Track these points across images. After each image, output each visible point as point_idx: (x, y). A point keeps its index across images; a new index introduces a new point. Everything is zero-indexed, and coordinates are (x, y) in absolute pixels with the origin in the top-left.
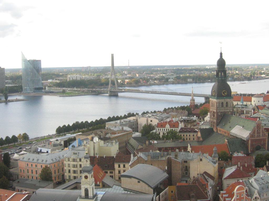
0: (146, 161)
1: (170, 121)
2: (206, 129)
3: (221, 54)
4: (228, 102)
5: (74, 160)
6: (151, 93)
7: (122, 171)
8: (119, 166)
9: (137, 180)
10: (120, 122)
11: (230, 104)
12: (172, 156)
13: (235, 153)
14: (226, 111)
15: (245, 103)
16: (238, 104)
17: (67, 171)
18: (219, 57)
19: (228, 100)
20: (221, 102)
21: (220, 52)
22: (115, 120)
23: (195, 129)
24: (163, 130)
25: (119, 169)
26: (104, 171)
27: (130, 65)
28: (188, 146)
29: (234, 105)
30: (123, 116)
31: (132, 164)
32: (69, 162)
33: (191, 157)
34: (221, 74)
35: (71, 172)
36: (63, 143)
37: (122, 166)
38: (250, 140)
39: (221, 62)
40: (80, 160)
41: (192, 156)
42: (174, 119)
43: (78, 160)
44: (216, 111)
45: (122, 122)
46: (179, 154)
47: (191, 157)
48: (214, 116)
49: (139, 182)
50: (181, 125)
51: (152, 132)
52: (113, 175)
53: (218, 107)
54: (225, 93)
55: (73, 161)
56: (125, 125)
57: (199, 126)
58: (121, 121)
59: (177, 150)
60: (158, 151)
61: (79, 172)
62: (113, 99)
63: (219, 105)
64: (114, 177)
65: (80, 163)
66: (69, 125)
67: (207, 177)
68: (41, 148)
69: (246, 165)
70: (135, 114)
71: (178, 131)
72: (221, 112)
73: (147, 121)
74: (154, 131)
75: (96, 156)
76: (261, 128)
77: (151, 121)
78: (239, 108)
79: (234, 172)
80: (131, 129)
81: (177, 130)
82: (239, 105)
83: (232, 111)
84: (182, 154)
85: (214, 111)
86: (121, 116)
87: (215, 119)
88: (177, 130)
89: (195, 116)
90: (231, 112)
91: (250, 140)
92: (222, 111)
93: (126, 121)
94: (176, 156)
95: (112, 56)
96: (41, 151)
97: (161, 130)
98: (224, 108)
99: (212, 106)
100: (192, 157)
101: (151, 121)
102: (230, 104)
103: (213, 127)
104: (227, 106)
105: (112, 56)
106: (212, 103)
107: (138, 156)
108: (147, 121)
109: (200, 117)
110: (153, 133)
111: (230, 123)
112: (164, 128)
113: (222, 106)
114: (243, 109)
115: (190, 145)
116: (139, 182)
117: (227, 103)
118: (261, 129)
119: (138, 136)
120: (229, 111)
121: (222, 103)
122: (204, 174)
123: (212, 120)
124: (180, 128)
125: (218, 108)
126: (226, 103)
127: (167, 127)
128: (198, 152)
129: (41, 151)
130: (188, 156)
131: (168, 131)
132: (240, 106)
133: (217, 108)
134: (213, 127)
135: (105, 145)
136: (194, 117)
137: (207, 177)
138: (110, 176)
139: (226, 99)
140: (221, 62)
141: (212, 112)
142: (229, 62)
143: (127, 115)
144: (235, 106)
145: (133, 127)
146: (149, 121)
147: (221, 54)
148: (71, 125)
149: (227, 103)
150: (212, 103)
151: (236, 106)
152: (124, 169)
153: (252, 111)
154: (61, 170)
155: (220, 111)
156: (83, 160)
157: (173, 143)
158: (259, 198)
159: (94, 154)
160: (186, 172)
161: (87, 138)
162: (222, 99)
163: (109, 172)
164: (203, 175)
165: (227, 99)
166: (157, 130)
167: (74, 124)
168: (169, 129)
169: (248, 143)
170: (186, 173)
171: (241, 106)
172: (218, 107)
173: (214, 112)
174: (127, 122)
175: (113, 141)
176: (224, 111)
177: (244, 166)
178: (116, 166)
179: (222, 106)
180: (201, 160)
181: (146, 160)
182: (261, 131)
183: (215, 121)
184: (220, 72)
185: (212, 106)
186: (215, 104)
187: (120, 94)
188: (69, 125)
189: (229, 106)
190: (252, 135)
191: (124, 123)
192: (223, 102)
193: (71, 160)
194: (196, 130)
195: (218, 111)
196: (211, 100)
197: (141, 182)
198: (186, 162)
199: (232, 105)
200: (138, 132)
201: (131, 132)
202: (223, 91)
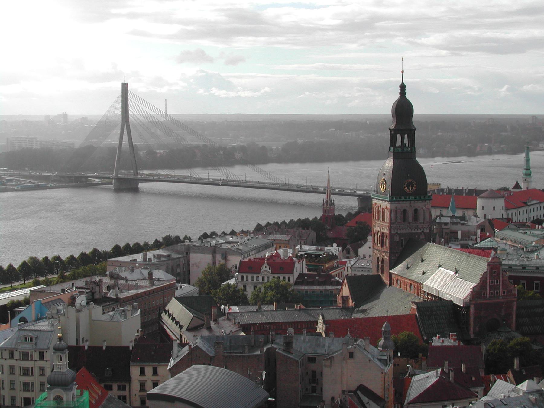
0: (211, 358)
1: (271, 257)
2: (362, 276)
3: (403, 87)
4: (419, 209)
5: (26, 356)
6: (222, 185)
7: (149, 384)
8: (142, 372)
10: (145, 259)
11: (424, 214)
12: (278, 346)
13: (434, 338)
14: (413, 231)
15: (459, 213)
16: (441, 216)
18: (397, 96)
19: (419, 205)
20: (402, 210)
21: (400, 84)
22: (131, 254)
23: (333, 277)
24: (253, 280)
25: (143, 378)
26: (102, 385)
27: (171, 111)
28: (318, 319)
29: (434, 216)
30: (151, 242)
31: (175, 366)
32: (12, 362)
33: (326, 348)
34: (403, 139)
37: (149, 370)
39: (403, 109)
40: (42, 356)
41: (327, 345)
42: (281, 251)
43: (36, 356)
44: (387, 232)
45: (150, 259)
46: (294, 341)
47: (326, 348)
50: (299, 268)
51: (225, 283)
52: (126, 393)
53: (393, 221)
54: (410, 188)
56: (157, 266)
57: (344, 268)
58: (146, 255)
60: (243, 334)
61: (37, 387)
62: (127, 197)
63: (396, 217)
64: (128, 398)
65: (42, 363)
66: (11, 266)
67: (365, 399)
69: (463, 369)
70: (182, 239)
71: (292, 281)
72: (401, 235)
74: (232, 282)
75: (81, 344)
76: (501, 274)
78: (446, 224)
79: (433, 385)
80: (173, 275)
81: (289, 278)
82: (445, 217)
83: (428, 231)
84: (304, 341)
85: (384, 231)
87: (387, 252)
88: (289, 278)
89: (335, 245)
90: (425, 234)
92: (404, 232)
94: (288, 345)
95: (125, 86)
97: (250, 279)
98: (409, 223)
99: (379, 218)
100: (329, 347)
102: (424, 214)
103: (380, 273)
104: (416, 218)
105: (125, 86)
107: (190, 346)
109: (348, 246)
110: (229, 286)
111: (422, 261)
112: (258, 275)
113: (405, 219)
114: (454, 228)
115: (323, 318)
117: (416, 211)
118: (501, 278)
119: (191, 296)
120: (421, 233)
122: (359, 392)
123: (377, 254)
124: (296, 274)
125: (393, 223)
126: (413, 210)
127: (265, 271)
128: (344, 335)
130: (319, 345)
131: (266, 281)
132: (448, 220)
133: (391, 223)
134: (380, 273)
135: (106, 317)
136: (332, 246)
137: (365, 399)
138: (119, 397)
139: (412, 202)
140: (403, 109)
141: (379, 234)
142: (420, 109)
143: (161, 241)
144: (436, 219)
145: (179, 271)
147: (403, 87)
148: (16, 266)
149: (416, 211)
151: (438, 221)
152: (155, 378)
153: (479, 231)
155: (399, 232)
156: (47, 356)
157: (279, 313)
159: (77, 340)
160: (313, 387)
161: (60, 298)
162: (403, 201)
163: (115, 387)
164: (355, 392)
165: (416, 202)
166: (240, 280)
167: (24, 264)
168: (268, 277)
169: (468, 315)
170: (314, 390)
171: (449, 218)
172: (393, 221)
173: (383, 234)
174: (163, 259)
175: (126, 308)
176: (408, 231)
177: (458, 370)
178: (135, 371)
179: (405, 219)
180: (351, 355)
181: (211, 355)
182: (501, 283)
184: (400, 134)
185: (379, 218)
186: (387, 215)
187: (141, 185)
188: (11, 266)
189: (421, 220)
190: (476, 293)
191: (155, 261)
192: (407, 209)
193: (16, 355)
194: (337, 278)
195: (393, 232)
196: (376, 204)
198: (312, 360)
199: (427, 216)
200: (189, 284)
201: (173, 285)
202: (408, 180)
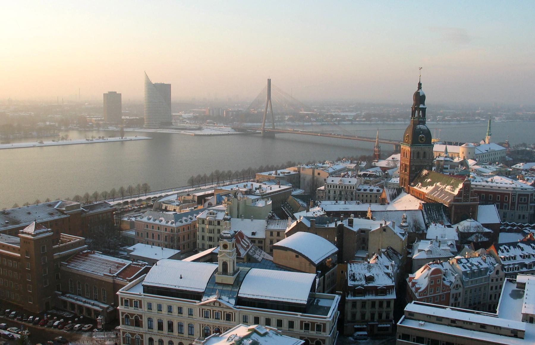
3: (420, 84)
7: (275, 240)
9: (294, 254)
12: (345, 223)
17: (200, 238)
19: (426, 149)
25: (271, 238)
30: (280, 166)
31: (289, 232)
32: (203, 226)
34: (419, 113)
35: (206, 238)
36: (196, 199)
38: (453, 207)
40: (219, 223)
43: (216, 223)
44: (408, 164)
48: (406, 171)
49: (297, 256)
52: (263, 245)
55: (209, 224)
59: (352, 215)
61: (216, 239)
63: (414, 156)
64: (263, 248)
65: (218, 227)
68: (167, 205)
73: (313, 173)
77: (319, 174)
86: (277, 166)
91: (453, 207)
93: (284, 173)
94: (351, 223)
95: (269, 81)
96: (166, 208)
101: (319, 174)
104: (424, 157)
105: (269, 81)
106: (404, 153)
108: (313, 173)
113: (418, 157)
116: (297, 256)
117: (425, 153)
121: (418, 153)
129: (166, 208)
145: (294, 181)
146: (316, 174)
147: (420, 84)
148: (208, 175)
149: (425, 153)
150: (404, 153)
152: (278, 238)
154: (192, 236)
156: (221, 223)
158: (462, 286)
173: (406, 165)
174: (286, 174)
179: (418, 157)
183: (407, 177)
186: (408, 155)
191: (281, 175)
193: (206, 222)
197: (299, 256)
200: (299, 188)
